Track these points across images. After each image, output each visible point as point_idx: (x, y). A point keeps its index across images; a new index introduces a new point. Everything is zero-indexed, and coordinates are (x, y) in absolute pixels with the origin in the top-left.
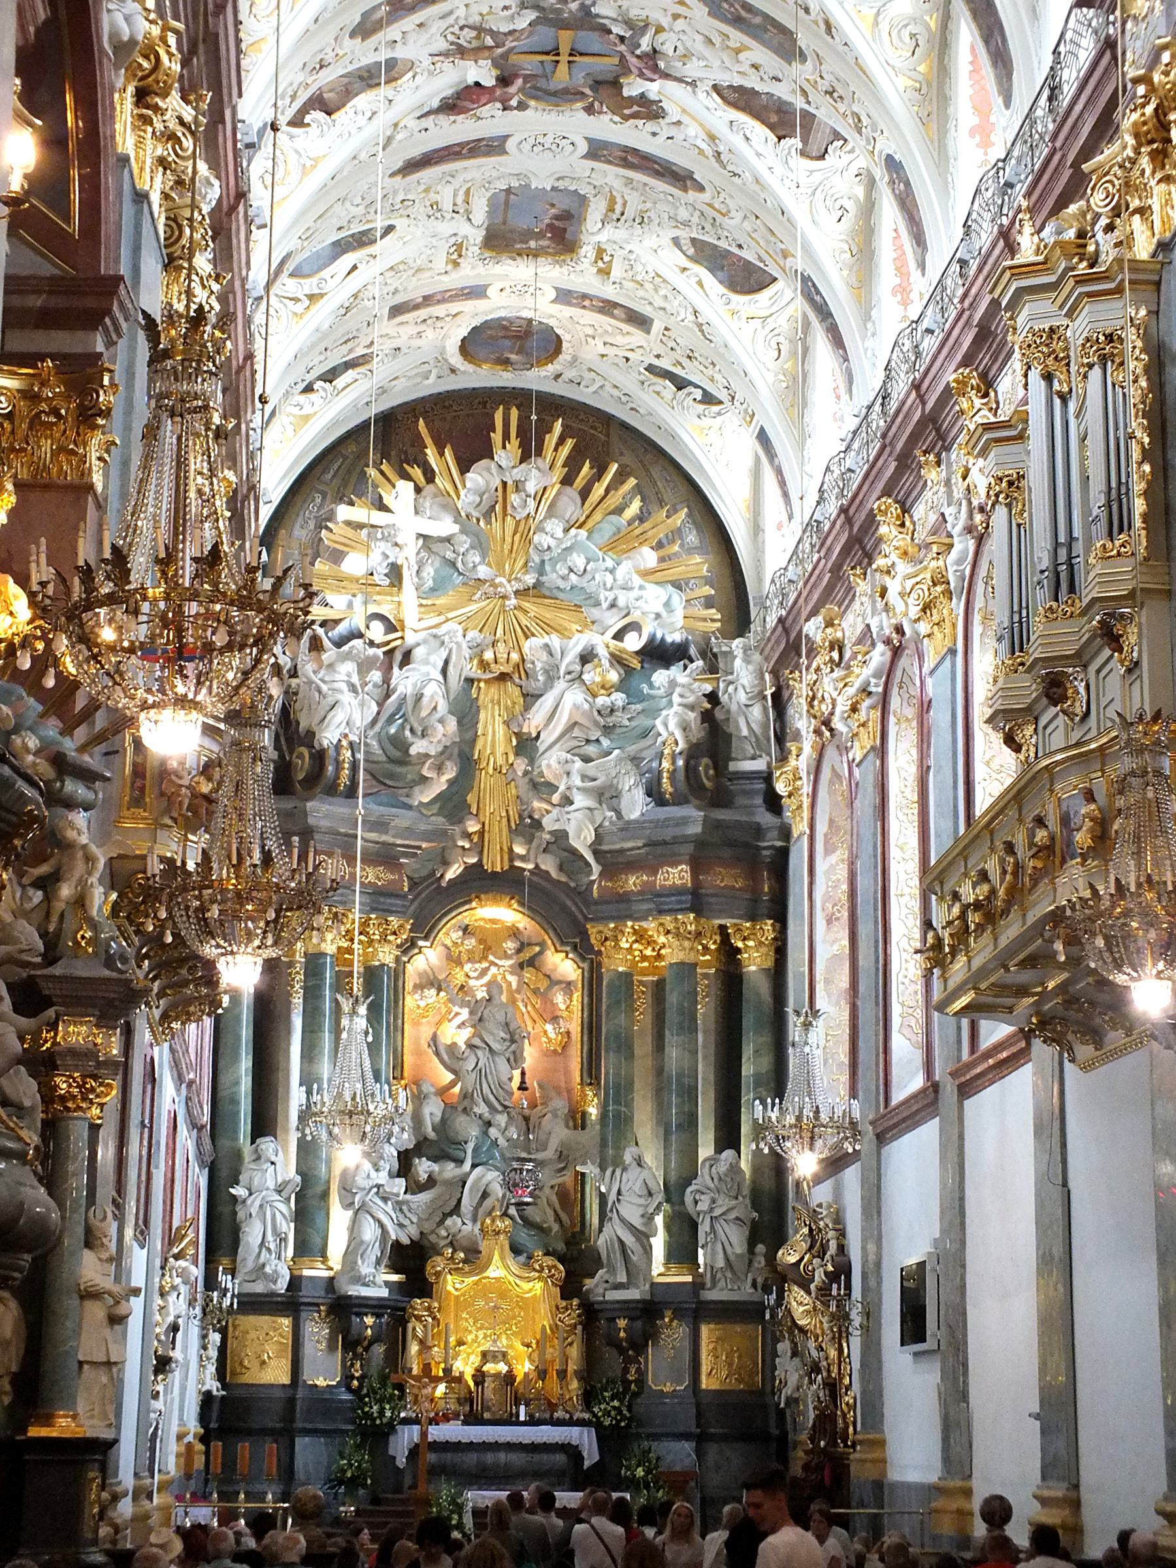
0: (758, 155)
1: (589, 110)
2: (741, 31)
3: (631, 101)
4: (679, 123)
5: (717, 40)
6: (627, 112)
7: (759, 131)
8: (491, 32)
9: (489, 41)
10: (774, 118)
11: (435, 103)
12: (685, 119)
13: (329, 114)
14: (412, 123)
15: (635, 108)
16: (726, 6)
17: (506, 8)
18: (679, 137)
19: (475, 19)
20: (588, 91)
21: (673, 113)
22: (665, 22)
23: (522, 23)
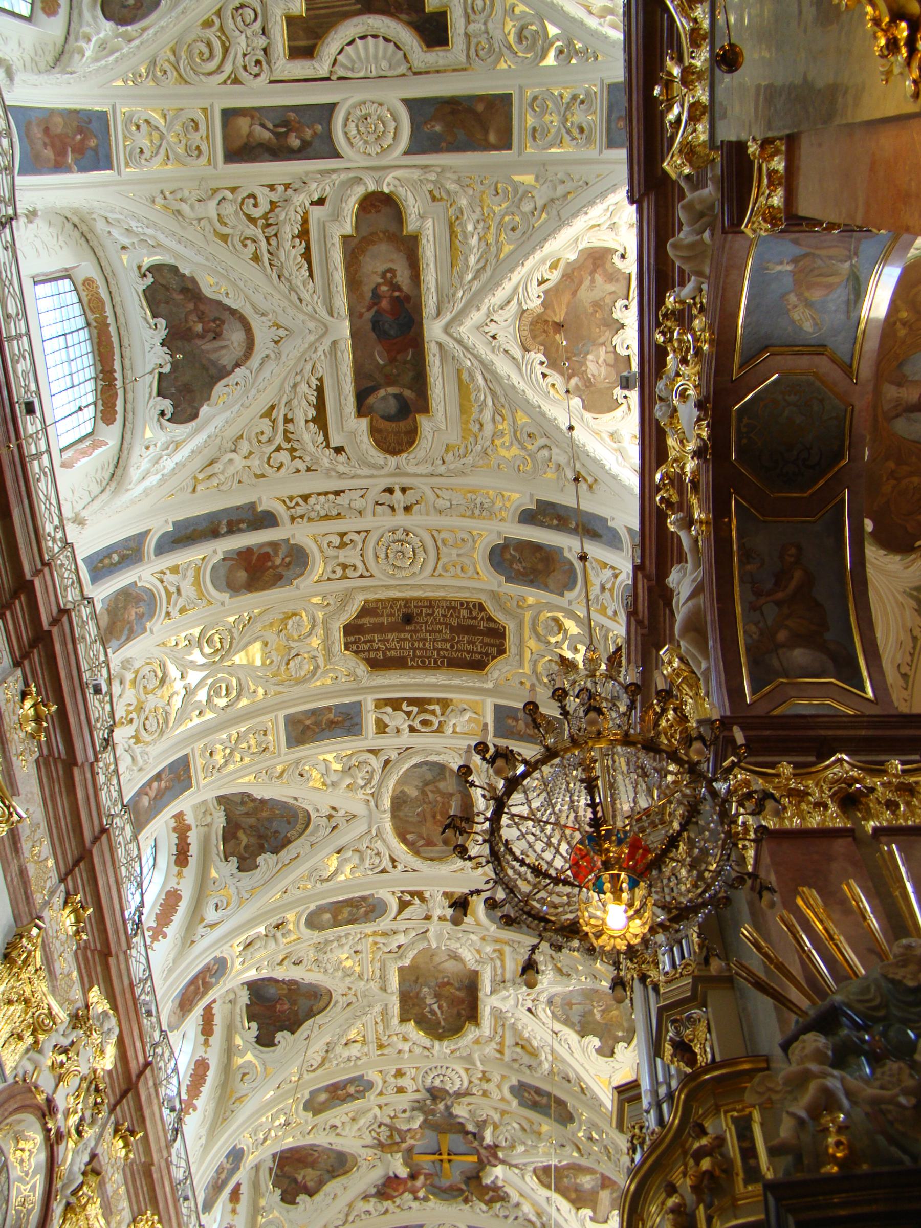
0: (566, 1220)
1: (466, 1201)
2: (538, 1112)
3: (488, 1188)
4: (518, 1205)
5: (527, 1126)
6: (487, 1198)
7: (565, 1205)
8: (399, 1131)
9: (397, 1139)
10: (573, 1196)
11: (374, 1191)
12: (522, 1200)
13: (311, 1195)
14: (362, 1206)
15: (491, 1193)
16: (526, 1095)
17: (404, 1111)
18: (520, 1214)
19: (387, 1120)
20: (464, 1187)
21: (515, 1197)
22: (496, 1117)
23: (416, 1125)
